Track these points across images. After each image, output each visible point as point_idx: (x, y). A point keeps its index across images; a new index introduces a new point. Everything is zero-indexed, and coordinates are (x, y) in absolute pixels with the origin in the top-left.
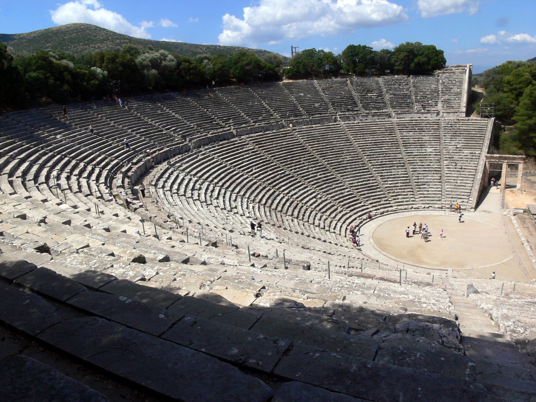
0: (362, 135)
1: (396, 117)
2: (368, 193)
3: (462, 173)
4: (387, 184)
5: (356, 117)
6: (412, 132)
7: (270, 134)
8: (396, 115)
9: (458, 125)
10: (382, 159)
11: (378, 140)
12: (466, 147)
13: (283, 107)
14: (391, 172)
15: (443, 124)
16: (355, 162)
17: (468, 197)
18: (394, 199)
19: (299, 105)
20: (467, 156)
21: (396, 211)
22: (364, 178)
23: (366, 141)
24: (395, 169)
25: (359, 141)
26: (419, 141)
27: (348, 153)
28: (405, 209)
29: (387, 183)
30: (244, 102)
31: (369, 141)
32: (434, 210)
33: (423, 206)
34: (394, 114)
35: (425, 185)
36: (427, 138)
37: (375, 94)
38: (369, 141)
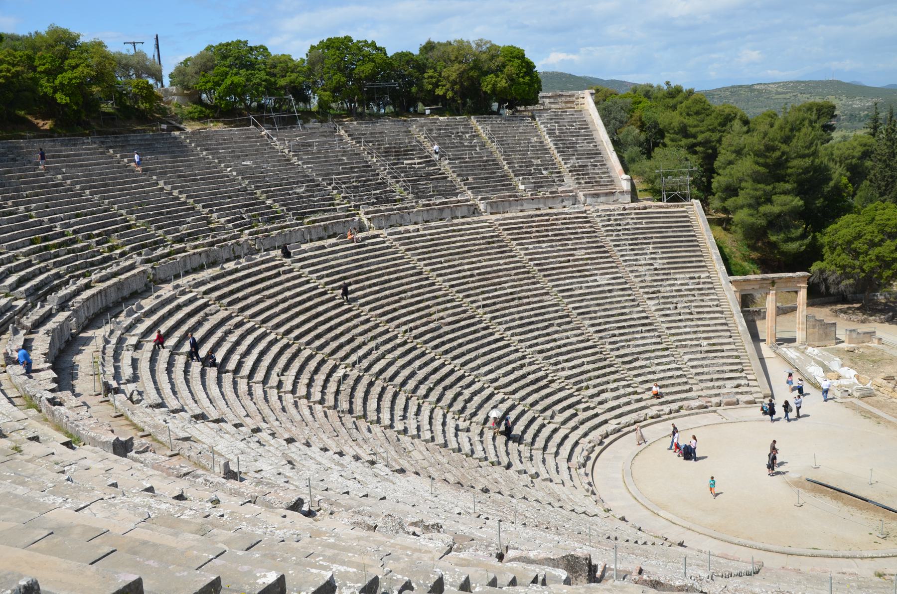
0: (443, 259)
1: (489, 211)
2: (542, 399)
3: (699, 323)
4: (563, 369)
5: (407, 217)
6: (544, 242)
7: (236, 271)
8: (489, 207)
9: (631, 222)
10: (519, 312)
11: (483, 267)
12: (675, 265)
13: (224, 198)
14: (555, 340)
15: (598, 219)
16: (468, 326)
17: (743, 374)
18: (601, 403)
19: (259, 192)
20: (687, 284)
21: (619, 430)
22: (510, 362)
23: (460, 271)
24: (556, 332)
25: (445, 274)
26: (569, 261)
27: (438, 304)
28: (635, 423)
29: (560, 366)
30: (113, 184)
31: (464, 271)
32: (693, 414)
33: (666, 409)
34: (482, 206)
35: (637, 359)
36: (580, 254)
37: (417, 161)
38: (464, 271)
